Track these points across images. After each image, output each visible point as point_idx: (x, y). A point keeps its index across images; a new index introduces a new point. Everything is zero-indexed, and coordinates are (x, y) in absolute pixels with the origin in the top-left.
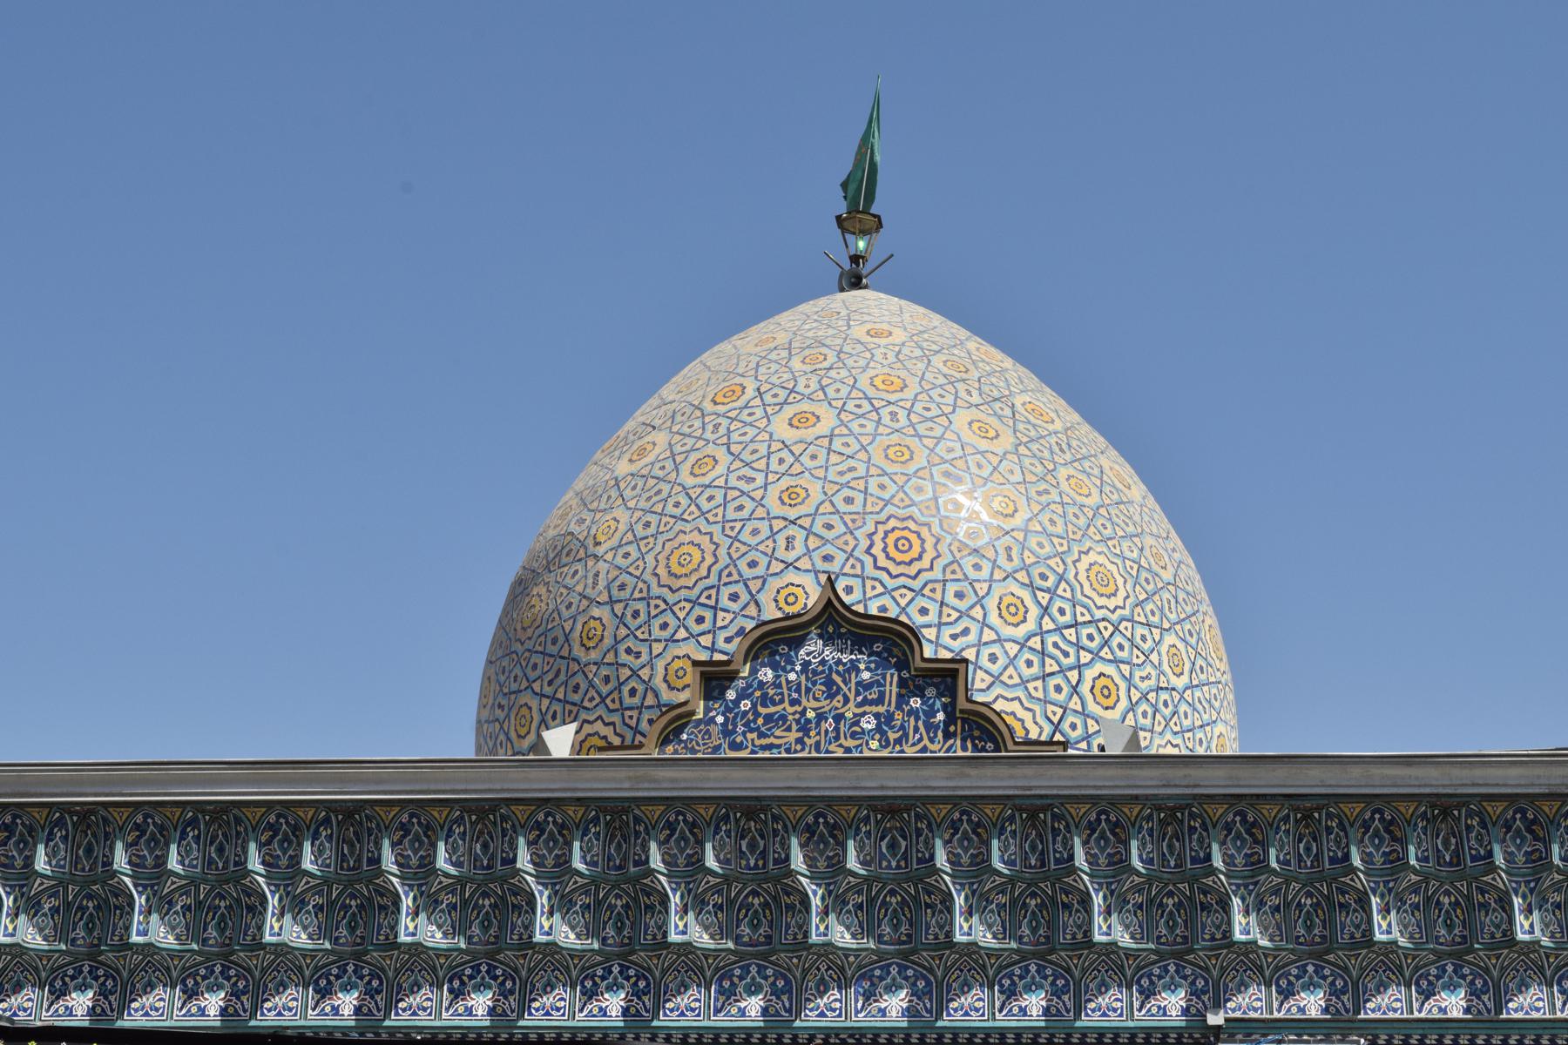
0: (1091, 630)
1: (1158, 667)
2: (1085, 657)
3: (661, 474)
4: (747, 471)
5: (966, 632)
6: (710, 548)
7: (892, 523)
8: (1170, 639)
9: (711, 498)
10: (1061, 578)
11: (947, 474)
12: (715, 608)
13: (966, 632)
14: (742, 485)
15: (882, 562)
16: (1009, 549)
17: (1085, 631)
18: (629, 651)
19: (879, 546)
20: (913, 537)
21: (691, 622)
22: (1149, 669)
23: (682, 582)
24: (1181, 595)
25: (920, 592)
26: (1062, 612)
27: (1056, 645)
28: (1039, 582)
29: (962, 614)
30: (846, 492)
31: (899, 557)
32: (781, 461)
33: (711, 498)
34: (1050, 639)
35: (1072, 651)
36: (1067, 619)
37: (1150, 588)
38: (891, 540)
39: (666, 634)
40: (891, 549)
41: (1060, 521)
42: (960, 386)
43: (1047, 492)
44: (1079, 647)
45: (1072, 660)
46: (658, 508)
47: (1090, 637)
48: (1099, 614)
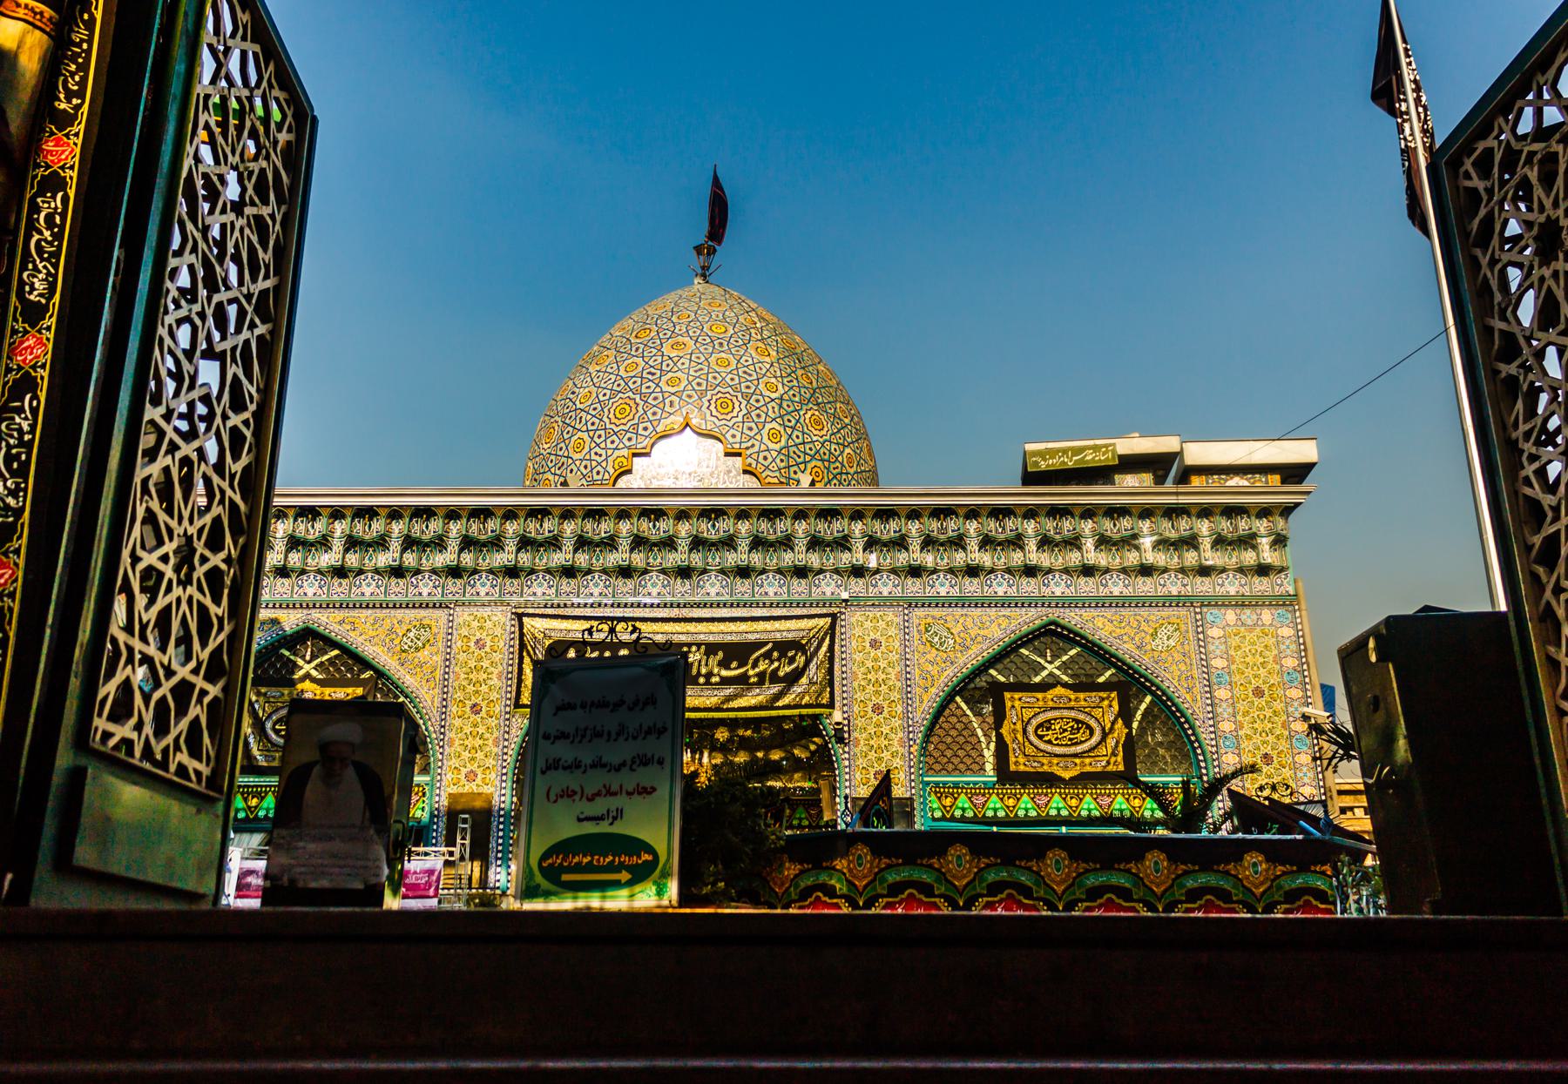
0: (811, 446)
1: (842, 464)
2: (808, 458)
3: (611, 371)
4: (652, 370)
5: (753, 446)
6: (634, 406)
7: (720, 395)
8: (848, 450)
9: (635, 382)
10: (798, 421)
11: (745, 372)
12: (637, 434)
13: (753, 446)
14: (650, 377)
15: (714, 413)
16: (773, 408)
17: (807, 446)
18: (596, 454)
19: (713, 405)
20: (729, 402)
21: (625, 440)
22: (838, 464)
23: (623, 421)
24: (854, 431)
25: (732, 427)
26: (798, 437)
27: (794, 453)
28: (787, 423)
29: (751, 438)
30: (698, 380)
31: (723, 411)
32: (668, 365)
33: (635, 382)
34: (792, 449)
35: (802, 455)
36: (800, 440)
37: (839, 426)
38: (719, 402)
39: (614, 446)
40: (719, 407)
41: (798, 395)
42: (752, 330)
43: (791, 381)
44: (806, 454)
45: (801, 460)
46: (610, 387)
47: (811, 449)
48: (815, 438)
